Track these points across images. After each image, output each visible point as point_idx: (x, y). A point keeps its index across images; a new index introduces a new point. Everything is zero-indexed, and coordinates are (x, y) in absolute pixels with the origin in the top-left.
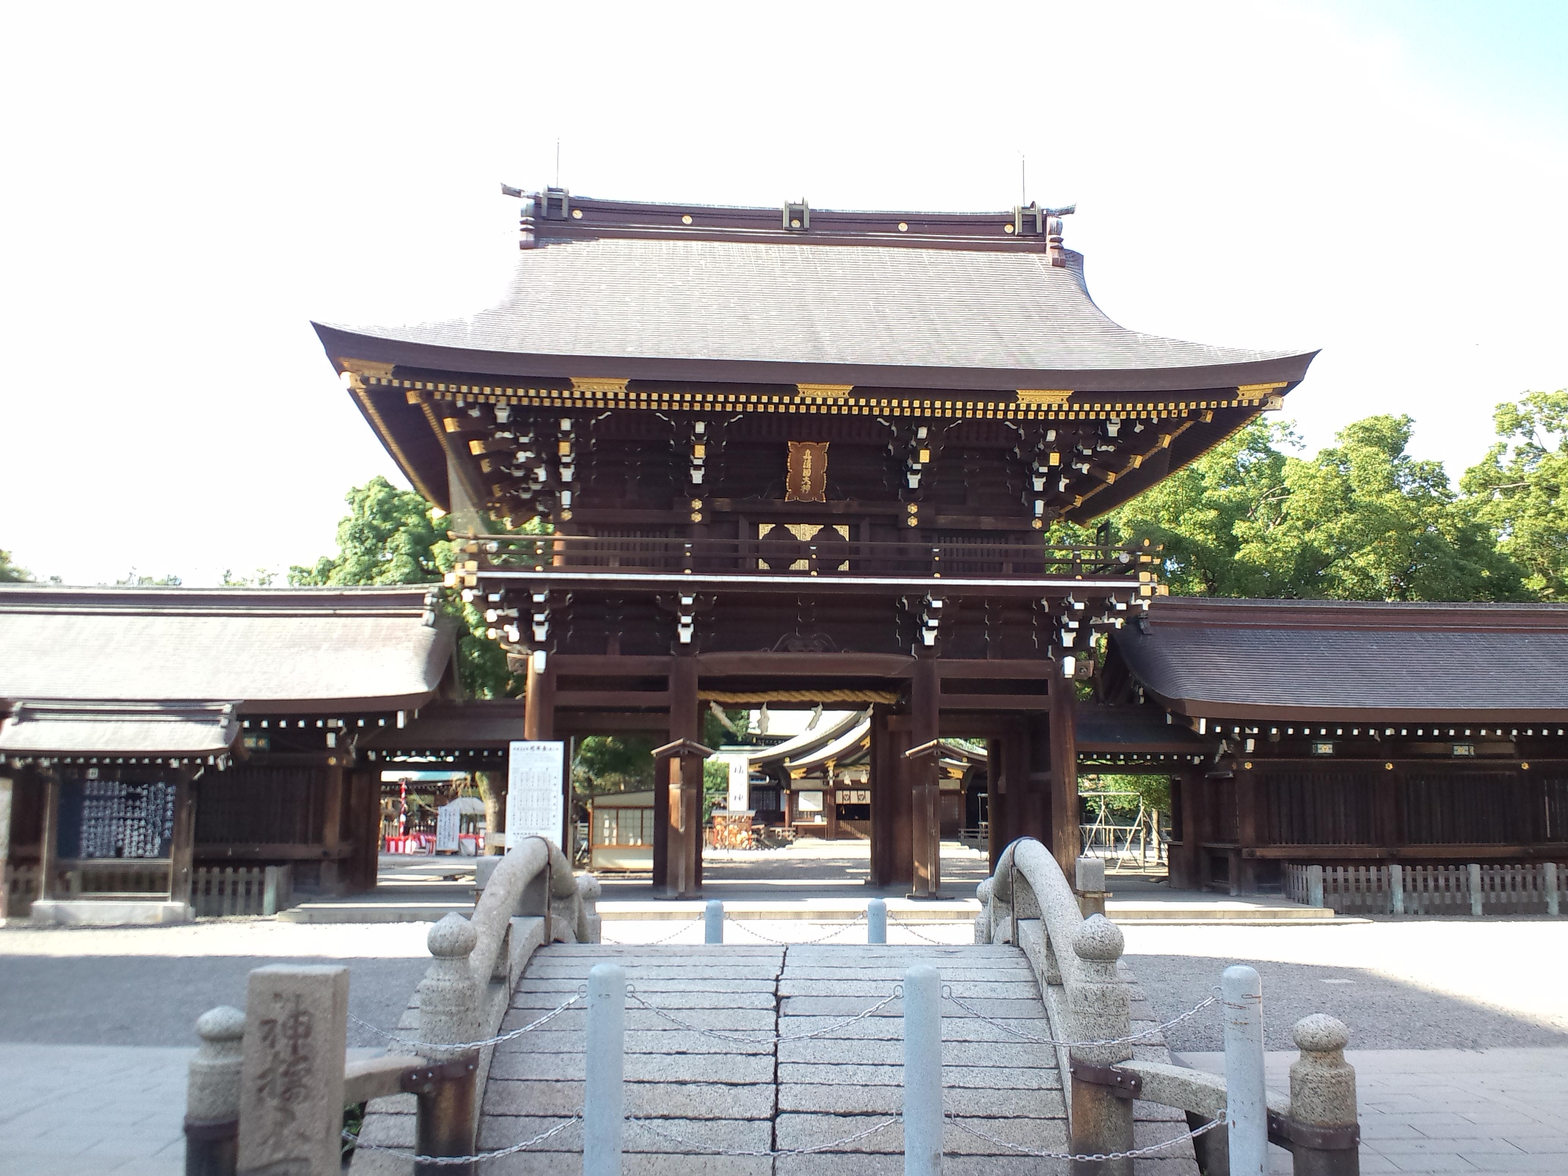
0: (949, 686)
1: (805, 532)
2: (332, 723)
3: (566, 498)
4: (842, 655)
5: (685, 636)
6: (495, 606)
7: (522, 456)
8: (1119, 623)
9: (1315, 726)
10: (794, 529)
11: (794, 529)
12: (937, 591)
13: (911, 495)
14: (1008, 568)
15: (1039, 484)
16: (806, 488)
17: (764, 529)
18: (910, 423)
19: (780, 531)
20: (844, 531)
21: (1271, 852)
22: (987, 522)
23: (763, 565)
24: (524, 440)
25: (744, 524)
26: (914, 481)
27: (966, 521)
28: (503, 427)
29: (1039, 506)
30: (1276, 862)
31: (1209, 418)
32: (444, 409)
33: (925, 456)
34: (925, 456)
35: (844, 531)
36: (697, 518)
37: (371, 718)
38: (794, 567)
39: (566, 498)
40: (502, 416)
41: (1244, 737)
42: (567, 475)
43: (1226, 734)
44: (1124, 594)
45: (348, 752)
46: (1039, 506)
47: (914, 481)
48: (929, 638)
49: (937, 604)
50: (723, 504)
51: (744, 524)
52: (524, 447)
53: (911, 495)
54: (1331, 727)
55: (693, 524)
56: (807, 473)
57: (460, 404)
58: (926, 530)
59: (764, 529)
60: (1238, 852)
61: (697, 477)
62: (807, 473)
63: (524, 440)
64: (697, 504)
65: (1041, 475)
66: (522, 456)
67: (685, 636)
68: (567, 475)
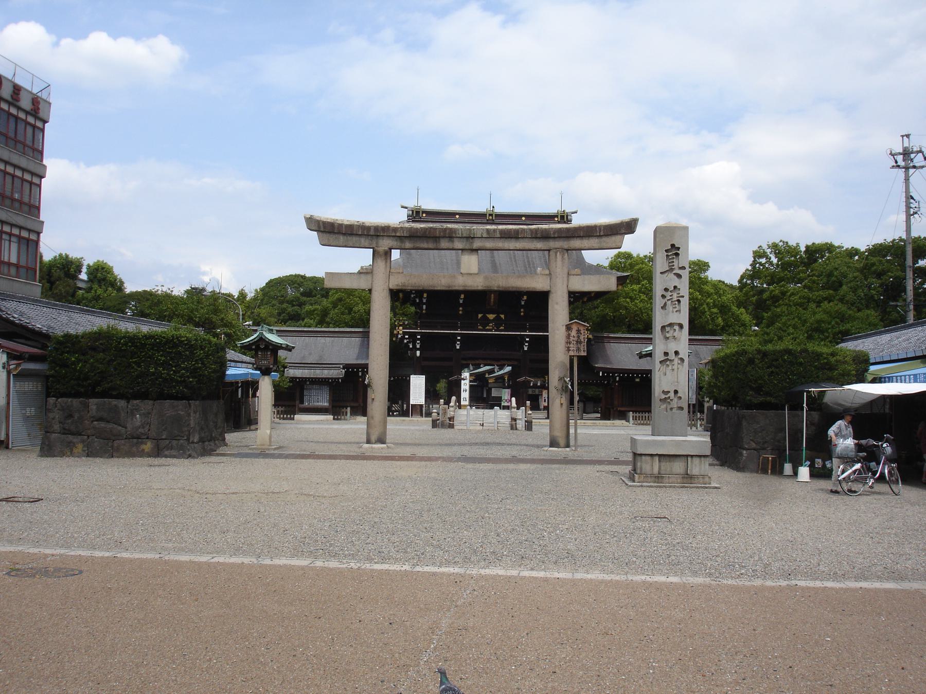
1: (491, 316)
3: (424, 307)
5: (458, 347)
12: (528, 336)
26: (523, 303)
35: (502, 316)
39: (424, 307)
42: (424, 301)
47: (523, 303)
48: (526, 349)
59: (480, 316)
61: (461, 301)
67: (458, 347)
68: (424, 301)
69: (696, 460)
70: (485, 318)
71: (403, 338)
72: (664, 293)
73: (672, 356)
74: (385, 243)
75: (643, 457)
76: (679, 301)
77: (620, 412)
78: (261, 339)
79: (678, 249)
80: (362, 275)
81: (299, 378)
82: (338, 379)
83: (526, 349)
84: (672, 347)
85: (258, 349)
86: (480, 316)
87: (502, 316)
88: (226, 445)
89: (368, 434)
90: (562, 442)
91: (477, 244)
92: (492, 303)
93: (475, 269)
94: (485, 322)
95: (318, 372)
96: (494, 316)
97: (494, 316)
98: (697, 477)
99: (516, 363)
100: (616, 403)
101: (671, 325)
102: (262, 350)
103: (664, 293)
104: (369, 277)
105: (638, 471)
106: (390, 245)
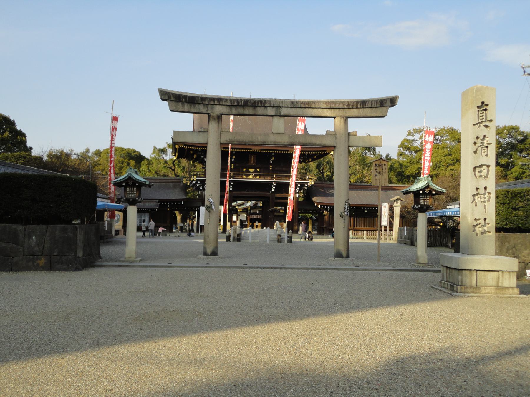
1: (251, 170)
4: (258, 192)
8: (306, 188)
10: (250, 170)
11: (250, 170)
13: (271, 164)
17: (244, 170)
18: (271, 153)
23: (244, 177)
26: (271, 162)
33: (273, 158)
34: (273, 158)
35: (258, 170)
44: (307, 183)
47: (271, 162)
48: (273, 190)
50: (237, 165)
69: (506, 275)
70: (247, 171)
71: (196, 183)
72: (476, 141)
73: (482, 191)
74: (218, 109)
75: (464, 272)
76: (487, 147)
78: (130, 178)
79: (487, 105)
80: (200, 133)
82: (155, 209)
83: (273, 190)
84: (482, 183)
85: (127, 185)
86: (244, 170)
87: (258, 170)
88: (100, 258)
89: (205, 248)
90: (344, 254)
91: (284, 111)
93: (282, 130)
94: (248, 174)
98: (508, 288)
101: (481, 166)
102: (130, 186)
103: (476, 141)
104: (205, 134)
105: (460, 284)
106: (221, 112)
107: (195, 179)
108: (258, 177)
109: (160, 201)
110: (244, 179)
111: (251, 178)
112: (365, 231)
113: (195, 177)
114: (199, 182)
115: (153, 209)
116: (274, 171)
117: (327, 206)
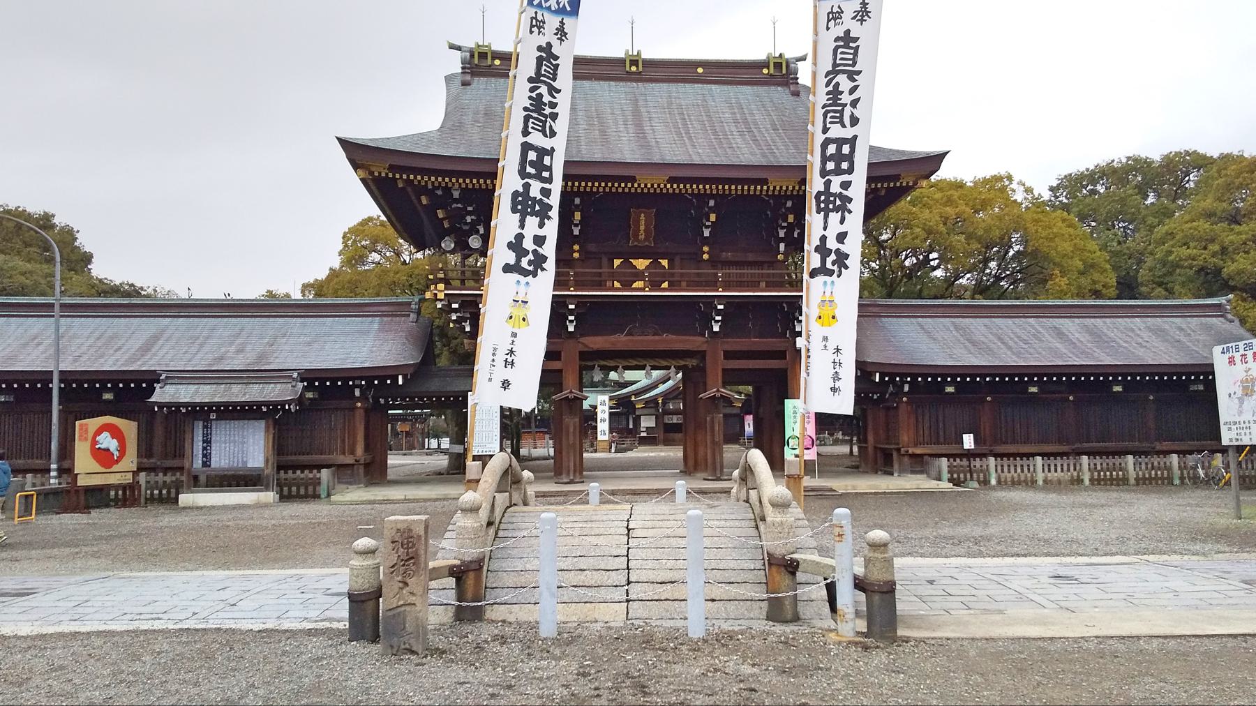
0: (729, 355)
1: (641, 264)
2: (357, 382)
5: (571, 328)
6: (455, 311)
7: (469, 219)
9: (944, 376)
13: (706, 241)
14: (763, 284)
15: (782, 234)
16: (642, 237)
17: (617, 262)
19: (627, 263)
20: (665, 263)
21: (918, 451)
22: (751, 257)
23: (617, 285)
24: (470, 209)
25: (605, 261)
26: (707, 233)
27: (740, 257)
28: (457, 201)
29: (782, 247)
30: (921, 456)
31: (883, 193)
32: (423, 190)
33: (713, 217)
34: (713, 217)
35: (665, 263)
36: (576, 255)
37: (382, 379)
38: (635, 285)
40: (456, 194)
41: (903, 382)
43: (892, 380)
45: (367, 399)
46: (782, 247)
47: (707, 233)
48: (716, 328)
49: (721, 307)
50: (592, 247)
51: (605, 261)
52: (470, 213)
53: (706, 241)
54: (954, 377)
55: (574, 259)
56: (642, 228)
57: (430, 186)
58: (714, 262)
59: (617, 262)
60: (898, 450)
61: (576, 231)
62: (642, 228)
63: (470, 209)
64: (576, 247)
65: (783, 228)
66: (469, 219)
67: (571, 328)
77: (913, 456)
81: (186, 405)
82: (283, 403)
83: (716, 328)
92: (642, 237)
95: (236, 389)
96: (647, 262)
97: (647, 262)
99: (691, 363)
100: (905, 438)
107: (441, 296)
108: (665, 285)
109: (310, 377)
110: (616, 291)
111: (640, 290)
112: (1039, 459)
113: (441, 286)
114: (455, 306)
115: (275, 404)
116: (714, 262)
117: (903, 376)
